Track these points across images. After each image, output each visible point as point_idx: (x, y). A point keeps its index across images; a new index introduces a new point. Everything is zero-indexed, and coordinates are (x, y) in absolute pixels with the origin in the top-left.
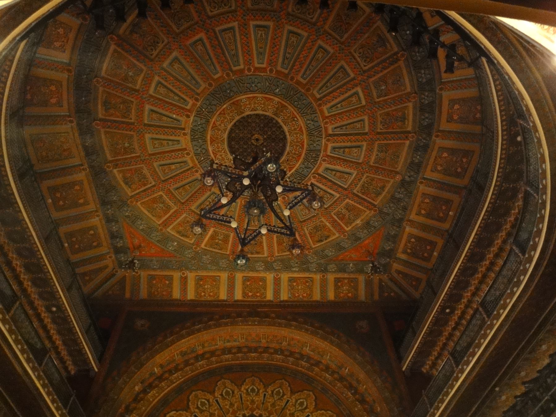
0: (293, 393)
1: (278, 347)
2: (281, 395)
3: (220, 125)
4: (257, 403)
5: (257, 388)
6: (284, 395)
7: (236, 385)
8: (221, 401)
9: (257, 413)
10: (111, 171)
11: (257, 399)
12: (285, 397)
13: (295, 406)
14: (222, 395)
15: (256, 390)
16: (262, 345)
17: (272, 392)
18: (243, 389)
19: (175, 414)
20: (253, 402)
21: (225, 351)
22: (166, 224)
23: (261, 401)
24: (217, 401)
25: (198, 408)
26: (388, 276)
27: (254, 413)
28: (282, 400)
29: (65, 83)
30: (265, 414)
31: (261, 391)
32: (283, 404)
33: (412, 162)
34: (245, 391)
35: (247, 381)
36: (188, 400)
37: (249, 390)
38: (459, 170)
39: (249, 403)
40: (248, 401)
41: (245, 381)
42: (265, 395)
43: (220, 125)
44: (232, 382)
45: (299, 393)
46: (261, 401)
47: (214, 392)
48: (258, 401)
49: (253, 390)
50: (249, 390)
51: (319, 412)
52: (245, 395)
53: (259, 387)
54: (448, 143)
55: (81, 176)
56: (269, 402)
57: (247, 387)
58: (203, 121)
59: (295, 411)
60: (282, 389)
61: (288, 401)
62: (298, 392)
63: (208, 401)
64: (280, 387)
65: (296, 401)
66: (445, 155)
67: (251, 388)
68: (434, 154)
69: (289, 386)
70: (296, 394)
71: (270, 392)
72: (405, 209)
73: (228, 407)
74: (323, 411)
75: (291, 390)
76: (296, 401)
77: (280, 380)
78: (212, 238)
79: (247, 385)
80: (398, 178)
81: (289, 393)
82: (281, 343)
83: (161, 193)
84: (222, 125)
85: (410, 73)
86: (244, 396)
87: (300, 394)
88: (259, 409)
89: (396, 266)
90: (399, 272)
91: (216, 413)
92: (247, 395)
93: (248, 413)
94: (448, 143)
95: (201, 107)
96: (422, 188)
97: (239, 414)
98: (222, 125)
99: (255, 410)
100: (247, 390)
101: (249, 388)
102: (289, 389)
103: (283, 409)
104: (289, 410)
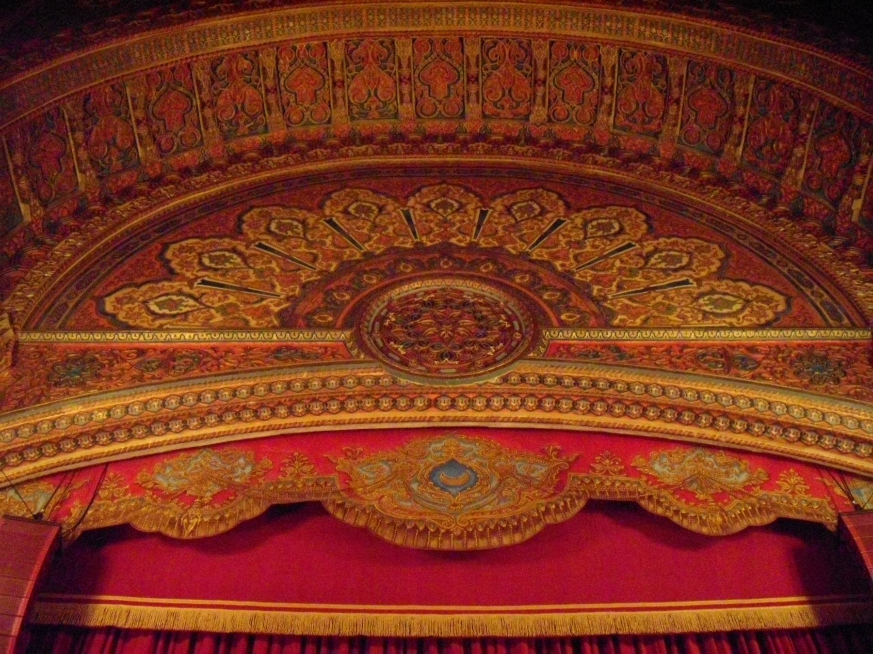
1: (515, 127)
7: (388, 196)
8: (344, 221)
11: (458, 218)
14: (346, 212)
16: (467, 125)
20: (445, 223)
21: (349, 140)
24: (330, 222)
25: (269, 231)
28: (542, 221)
32: (546, 226)
34: (418, 206)
35: (424, 190)
36: (240, 220)
37: (433, 205)
39: (432, 225)
42: (483, 214)
44: (375, 191)
47: (321, 206)
51: (661, 240)
59: (585, 238)
62: (589, 208)
63: (304, 223)
69: (560, 196)
70: (584, 212)
73: (365, 231)
74: (673, 239)
79: (426, 196)
82: (527, 118)
86: (417, 214)
91: (328, 241)
99: (454, 236)
100: (428, 205)
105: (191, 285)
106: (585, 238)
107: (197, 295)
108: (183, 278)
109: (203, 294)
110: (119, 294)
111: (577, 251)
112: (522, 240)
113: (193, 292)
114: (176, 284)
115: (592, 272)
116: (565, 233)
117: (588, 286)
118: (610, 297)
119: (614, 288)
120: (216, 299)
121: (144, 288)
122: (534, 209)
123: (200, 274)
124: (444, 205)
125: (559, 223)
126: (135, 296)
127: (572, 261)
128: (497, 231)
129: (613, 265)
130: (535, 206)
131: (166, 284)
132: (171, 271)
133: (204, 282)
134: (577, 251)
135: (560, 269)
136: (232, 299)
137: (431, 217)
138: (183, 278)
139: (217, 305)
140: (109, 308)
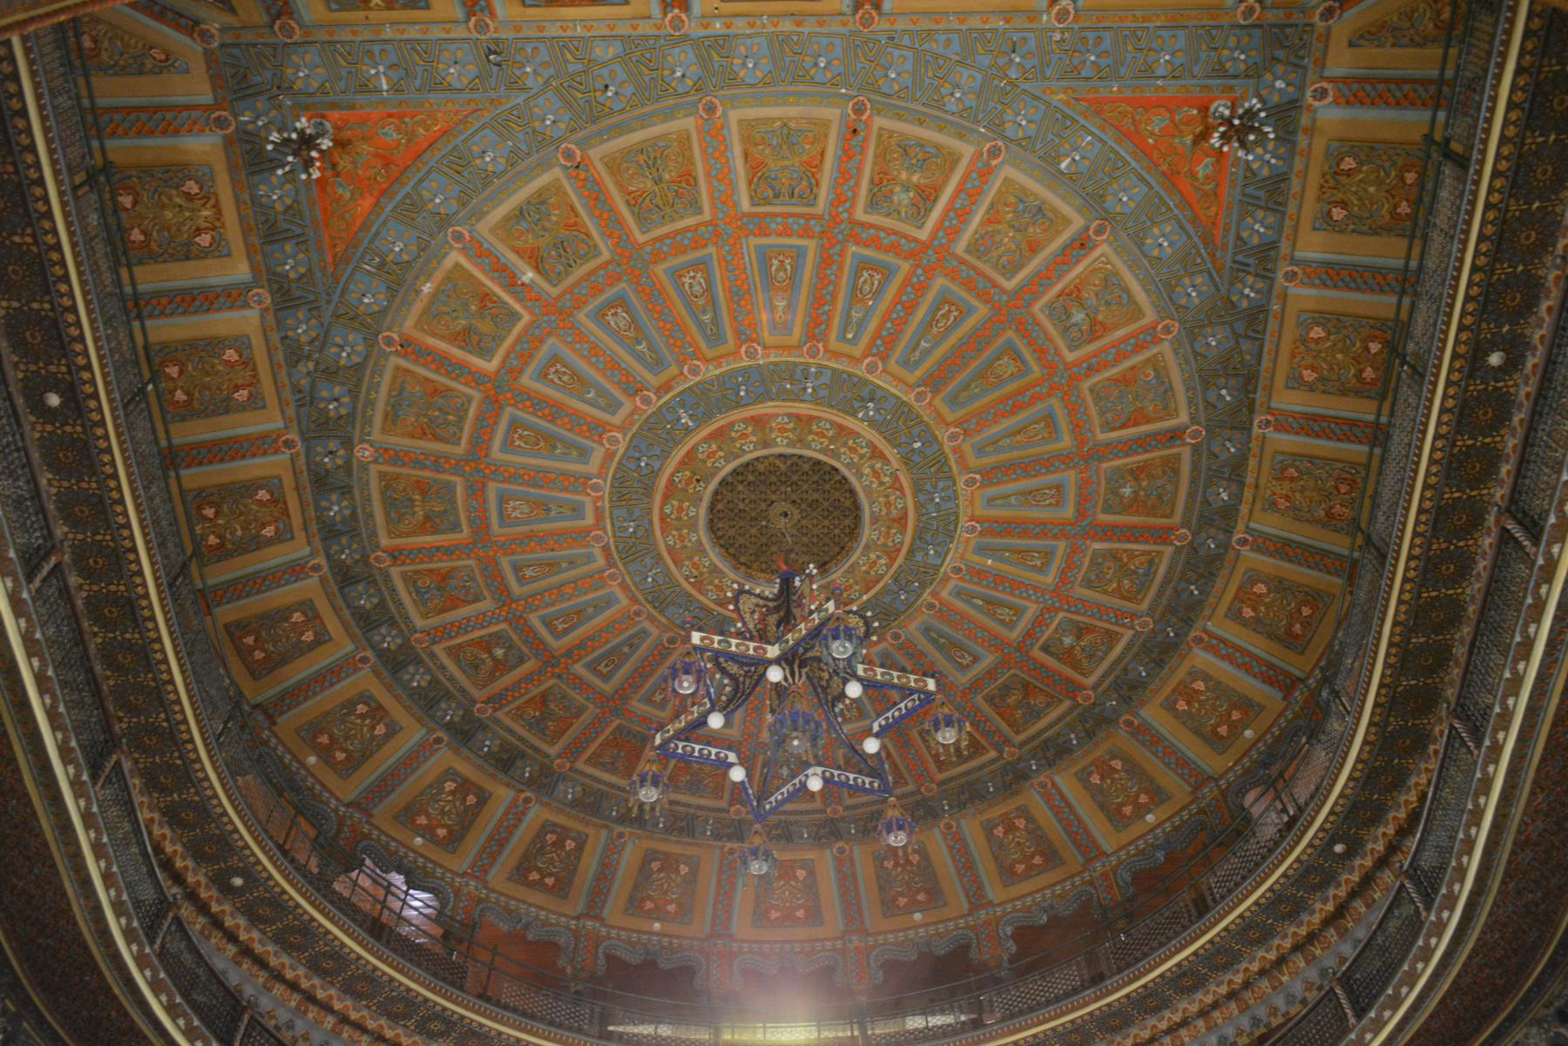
3: (879, 557)
10: (1194, 419)
22: (1082, 243)
26: (205, 36)
29: (1222, 609)
33: (346, 491)
38: (209, 512)
43: (879, 557)
54: (275, 557)
55: (1290, 401)
58: (919, 556)
66: (269, 531)
68: (296, 521)
72: (295, 355)
78: (927, 196)
80: (364, 453)
83: (1070, 357)
84: (873, 556)
85: (452, 679)
89: (195, 88)
90: (168, 62)
94: (275, 557)
95: (923, 586)
96: (269, 421)
98: (873, 556)
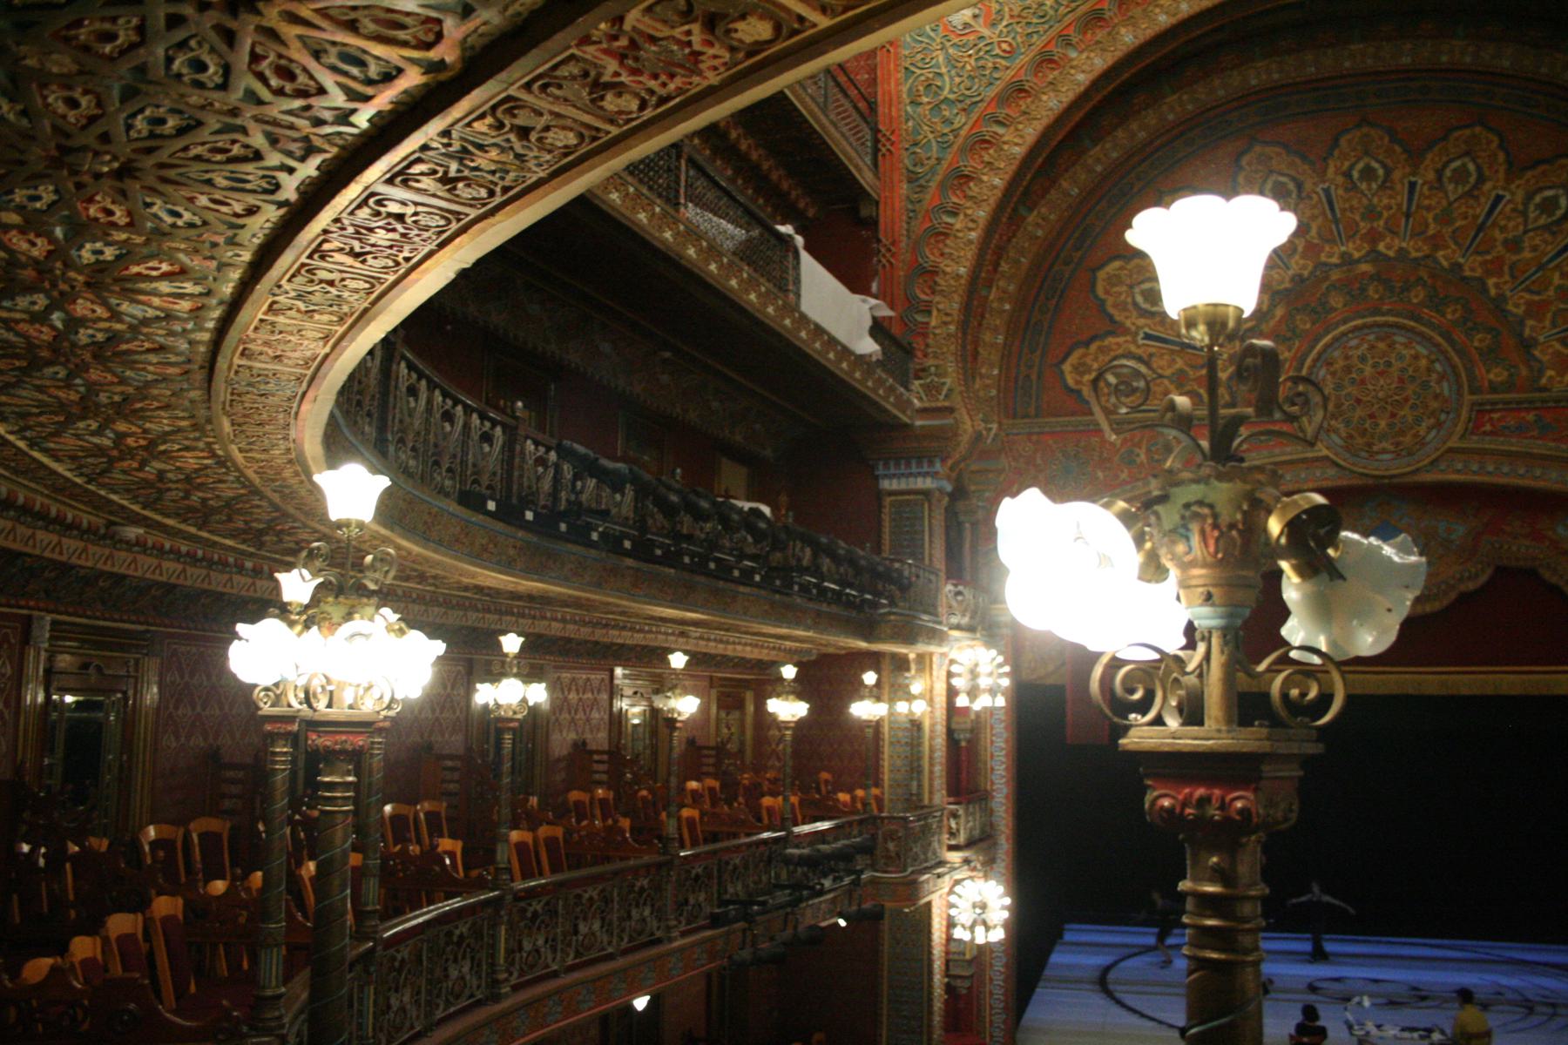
0: (1515, 169)
2: (1472, 180)
4: (1386, 214)
5: (1384, 166)
6: (1481, 179)
9: (1389, 247)
11: (1385, 201)
12: (1488, 186)
13: (1524, 214)
15: (1381, 172)
17: (1439, 173)
18: (1331, 171)
19: (1121, 268)
23: (1399, 206)
27: (1381, 247)
28: (1477, 198)
30: (1417, 250)
31: (1397, 175)
32: (1481, 211)
34: (1340, 179)
35: (1343, 142)
37: (1355, 174)
39: (1358, 218)
40: (1352, 209)
41: (1335, 143)
42: (1412, 185)
45: (1540, 169)
46: (1399, 206)
48: (1389, 208)
49: (1368, 173)
50: (1355, 174)
52: (1340, 192)
53: (1388, 162)
56: (1429, 208)
57: (1347, 164)
59: (1525, 232)
60: (1474, 160)
61: (1499, 198)
64: (1467, 153)
65: (1529, 197)
67: (1360, 165)
71: (1431, 176)
75: (1509, 163)
76: (1529, 197)
77: (1466, 127)
81: (1502, 170)
87: (1544, 173)
88: (1394, 233)
92: (1347, 190)
93: (1358, 250)
97: (1331, 255)
99: (1382, 237)
101: (1352, 167)
102: (1501, 157)
103: (1480, 228)
104: (1503, 229)
105: (1134, 342)
106: (1525, 232)
107: (1145, 357)
108: (1126, 331)
109: (1151, 355)
110: (1074, 358)
111: (1514, 258)
112: (1456, 243)
113: (1139, 352)
114: (1121, 340)
115: (1527, 296)
116: (1503, 223)
117: (1522, 323)
118: (1541, 339)
119: (1547, 323)
120: (1163, 363)
121: (1093, 347)
122: (1469, 174)
123: (1141, 322)
124: (1368, 173)
125: (1499, 198)
126: (1088, 360)
127: (1507, 277)
128: (1427, 226)
129: (1550, 283)
130: (1471, 167)
131: (1111, 340)
132: (1111, 317)
133: (1148, 337)
134: (1514, 258)
135: (1493, 292)
136: (1180, 364)
137: (1355, 202)
138: (1126, 331)
139: (1168, 372)
140: (1070, 381)
